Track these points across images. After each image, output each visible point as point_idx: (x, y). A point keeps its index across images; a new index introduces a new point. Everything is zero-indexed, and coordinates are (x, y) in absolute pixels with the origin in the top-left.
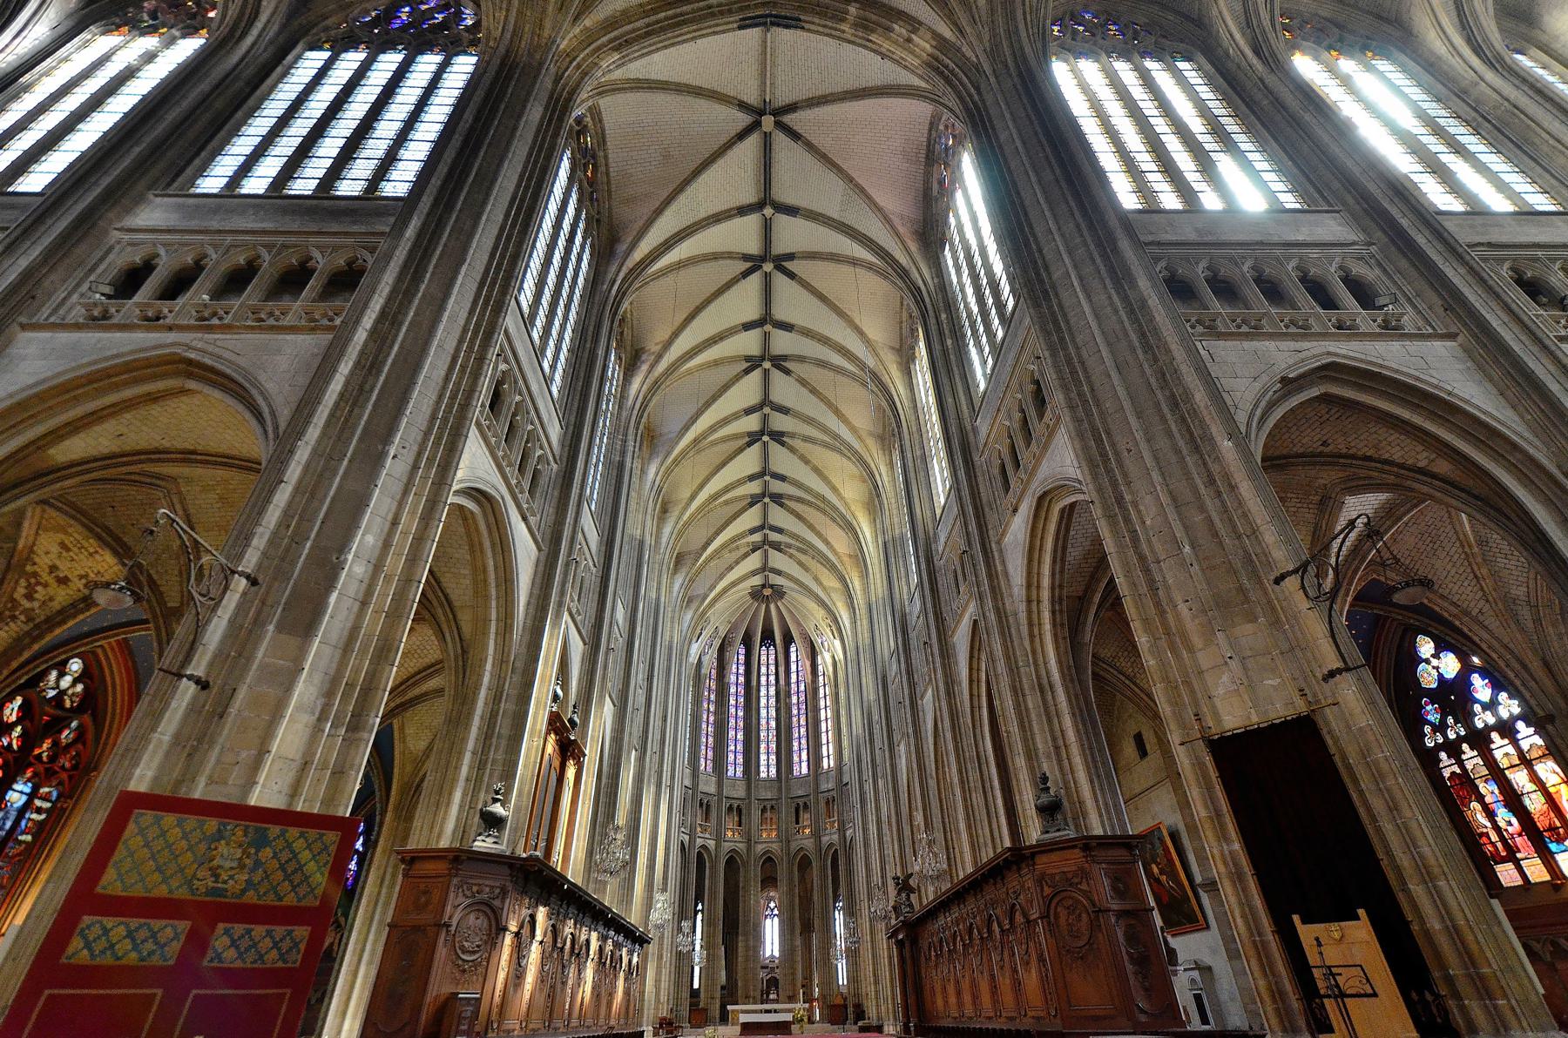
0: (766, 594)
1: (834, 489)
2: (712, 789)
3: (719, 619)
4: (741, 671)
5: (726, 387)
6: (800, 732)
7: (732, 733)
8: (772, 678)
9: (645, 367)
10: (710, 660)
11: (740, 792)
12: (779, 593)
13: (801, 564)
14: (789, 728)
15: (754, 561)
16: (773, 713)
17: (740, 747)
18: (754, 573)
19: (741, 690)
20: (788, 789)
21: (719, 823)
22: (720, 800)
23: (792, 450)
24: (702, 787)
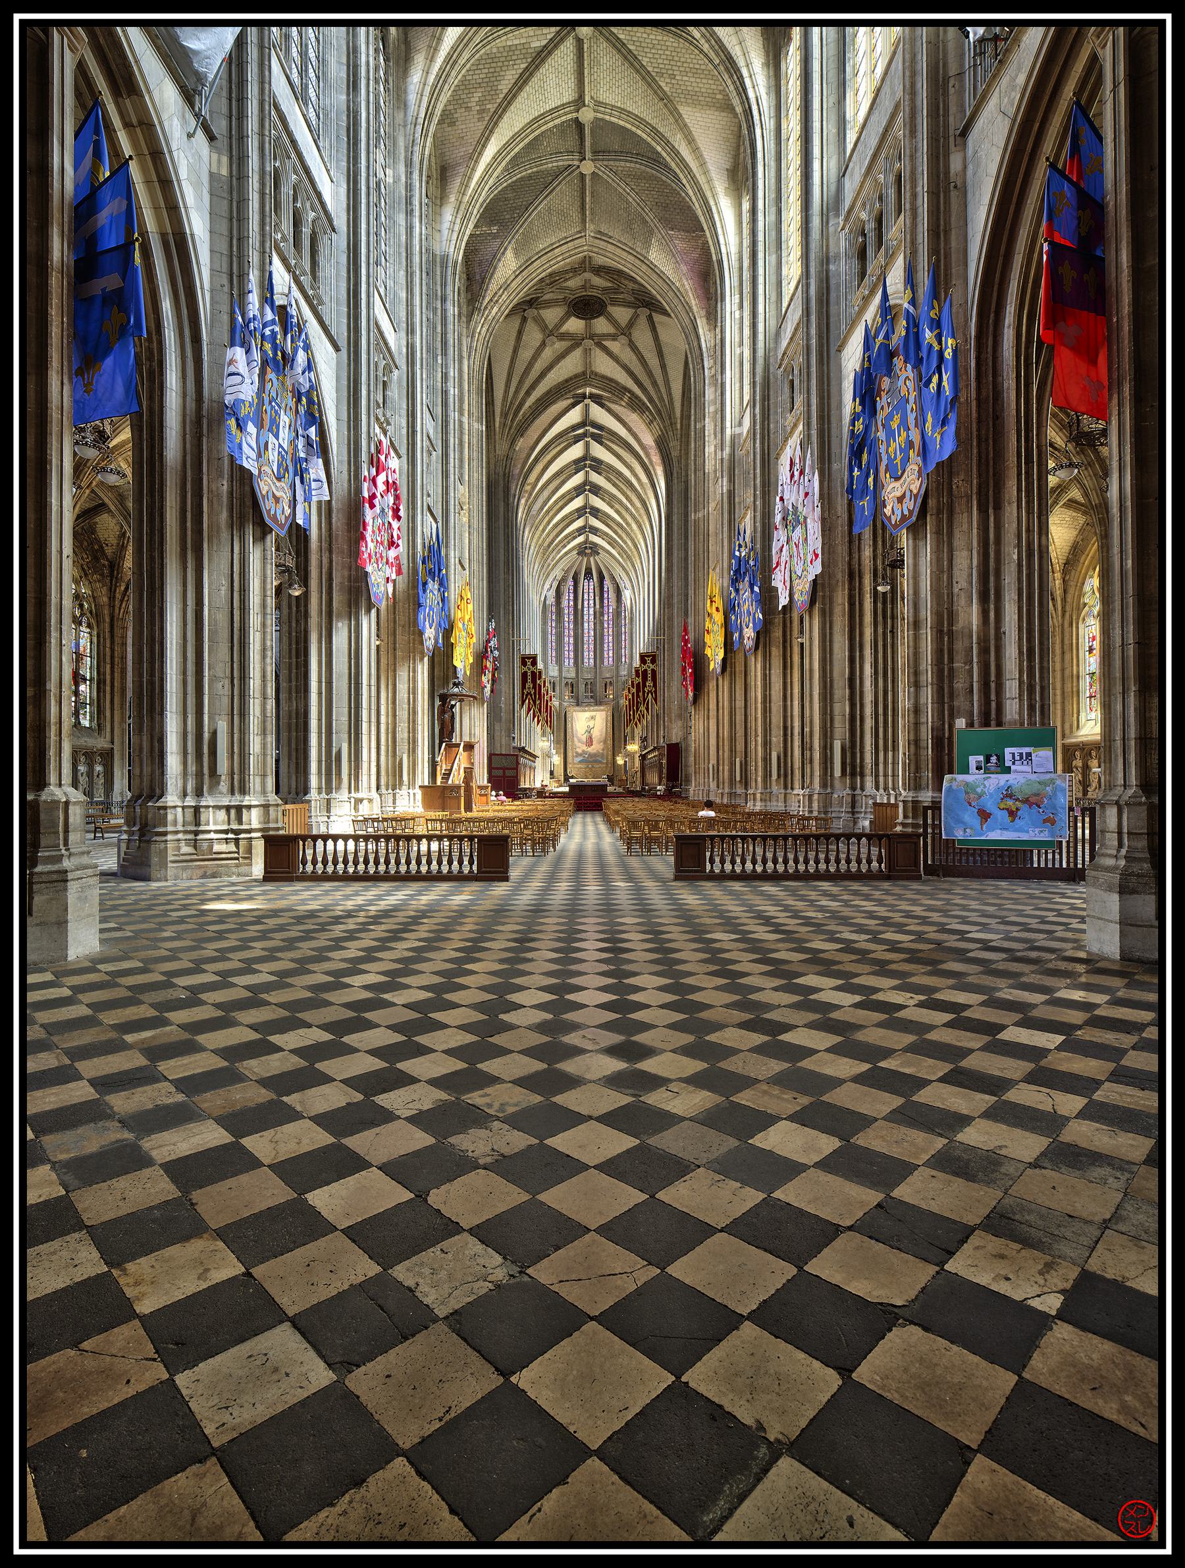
0: (588, 550)
1: (627, 524)
2: (556, 673)
3: (558, 573)
4: (572, 595)
5: (563, 483)
6: (609, 639)
7: (566, 639)
8: (591, 602)
9: (523, 501)
10: (552, 593)
11: (573, 675)
12: (594, 549)
13: (609, 543)
14: (602, 635)
15: (581, 539)
16: (592, 624)
17: (571, 647)
18: (579, 545)
19: (571, 609)
20: (601, 672)
21: (561, 693)
22: (561, 680)
23: (603, 500)
24: (551, 673)
